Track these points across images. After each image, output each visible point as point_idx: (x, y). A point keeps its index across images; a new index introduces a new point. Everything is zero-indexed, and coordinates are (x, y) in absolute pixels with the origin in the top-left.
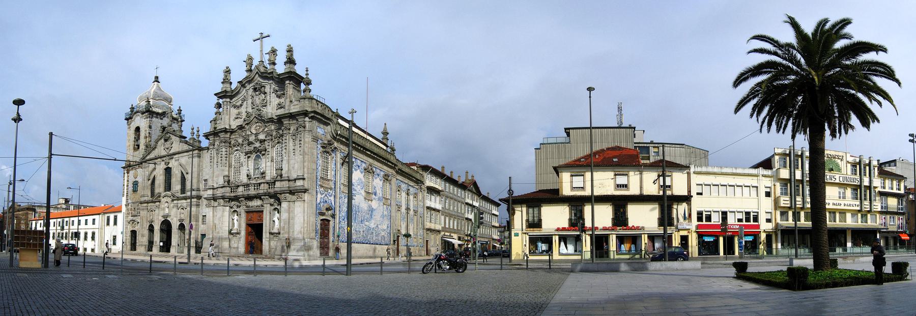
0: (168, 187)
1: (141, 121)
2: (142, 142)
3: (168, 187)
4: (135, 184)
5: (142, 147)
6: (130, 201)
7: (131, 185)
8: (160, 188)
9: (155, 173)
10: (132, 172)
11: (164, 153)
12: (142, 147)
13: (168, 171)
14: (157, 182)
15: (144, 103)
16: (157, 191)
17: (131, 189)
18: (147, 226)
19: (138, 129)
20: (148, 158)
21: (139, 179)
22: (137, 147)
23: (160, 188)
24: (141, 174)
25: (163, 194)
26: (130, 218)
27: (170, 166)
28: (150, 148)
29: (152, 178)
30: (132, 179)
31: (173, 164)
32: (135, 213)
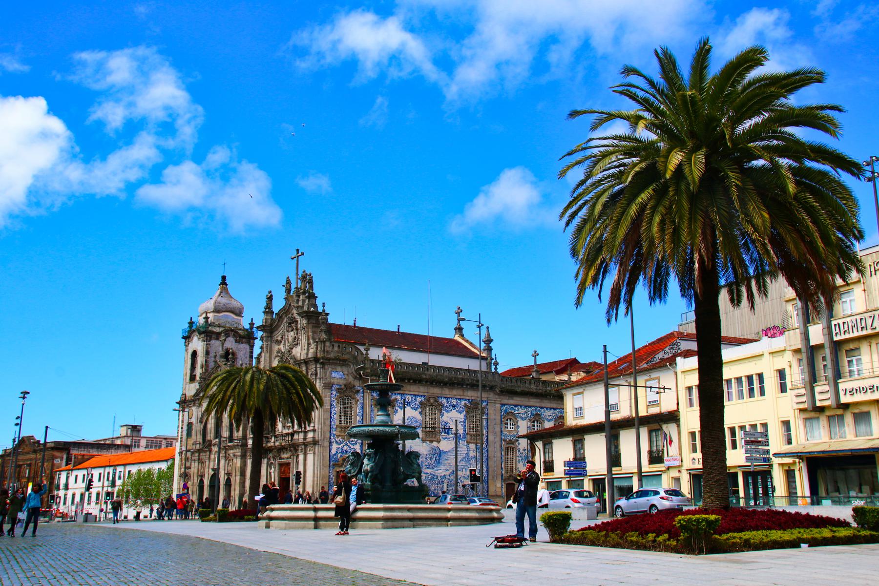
1: (197, 344)
2: (199, 371)
4: (190, 425)
7: (185, 428)
8: (210, 436)
10: (187, 410)
12: (198, 378)
14: (209, 426)
15: (201, 321)
16: (208, 438)
17: (185, 432)
18: (196, 480)
19: (194, 354)
21: (193, 420)
22: (192, 378)
23: (210, 436)
24: (196, 412)
25: (214, 442)
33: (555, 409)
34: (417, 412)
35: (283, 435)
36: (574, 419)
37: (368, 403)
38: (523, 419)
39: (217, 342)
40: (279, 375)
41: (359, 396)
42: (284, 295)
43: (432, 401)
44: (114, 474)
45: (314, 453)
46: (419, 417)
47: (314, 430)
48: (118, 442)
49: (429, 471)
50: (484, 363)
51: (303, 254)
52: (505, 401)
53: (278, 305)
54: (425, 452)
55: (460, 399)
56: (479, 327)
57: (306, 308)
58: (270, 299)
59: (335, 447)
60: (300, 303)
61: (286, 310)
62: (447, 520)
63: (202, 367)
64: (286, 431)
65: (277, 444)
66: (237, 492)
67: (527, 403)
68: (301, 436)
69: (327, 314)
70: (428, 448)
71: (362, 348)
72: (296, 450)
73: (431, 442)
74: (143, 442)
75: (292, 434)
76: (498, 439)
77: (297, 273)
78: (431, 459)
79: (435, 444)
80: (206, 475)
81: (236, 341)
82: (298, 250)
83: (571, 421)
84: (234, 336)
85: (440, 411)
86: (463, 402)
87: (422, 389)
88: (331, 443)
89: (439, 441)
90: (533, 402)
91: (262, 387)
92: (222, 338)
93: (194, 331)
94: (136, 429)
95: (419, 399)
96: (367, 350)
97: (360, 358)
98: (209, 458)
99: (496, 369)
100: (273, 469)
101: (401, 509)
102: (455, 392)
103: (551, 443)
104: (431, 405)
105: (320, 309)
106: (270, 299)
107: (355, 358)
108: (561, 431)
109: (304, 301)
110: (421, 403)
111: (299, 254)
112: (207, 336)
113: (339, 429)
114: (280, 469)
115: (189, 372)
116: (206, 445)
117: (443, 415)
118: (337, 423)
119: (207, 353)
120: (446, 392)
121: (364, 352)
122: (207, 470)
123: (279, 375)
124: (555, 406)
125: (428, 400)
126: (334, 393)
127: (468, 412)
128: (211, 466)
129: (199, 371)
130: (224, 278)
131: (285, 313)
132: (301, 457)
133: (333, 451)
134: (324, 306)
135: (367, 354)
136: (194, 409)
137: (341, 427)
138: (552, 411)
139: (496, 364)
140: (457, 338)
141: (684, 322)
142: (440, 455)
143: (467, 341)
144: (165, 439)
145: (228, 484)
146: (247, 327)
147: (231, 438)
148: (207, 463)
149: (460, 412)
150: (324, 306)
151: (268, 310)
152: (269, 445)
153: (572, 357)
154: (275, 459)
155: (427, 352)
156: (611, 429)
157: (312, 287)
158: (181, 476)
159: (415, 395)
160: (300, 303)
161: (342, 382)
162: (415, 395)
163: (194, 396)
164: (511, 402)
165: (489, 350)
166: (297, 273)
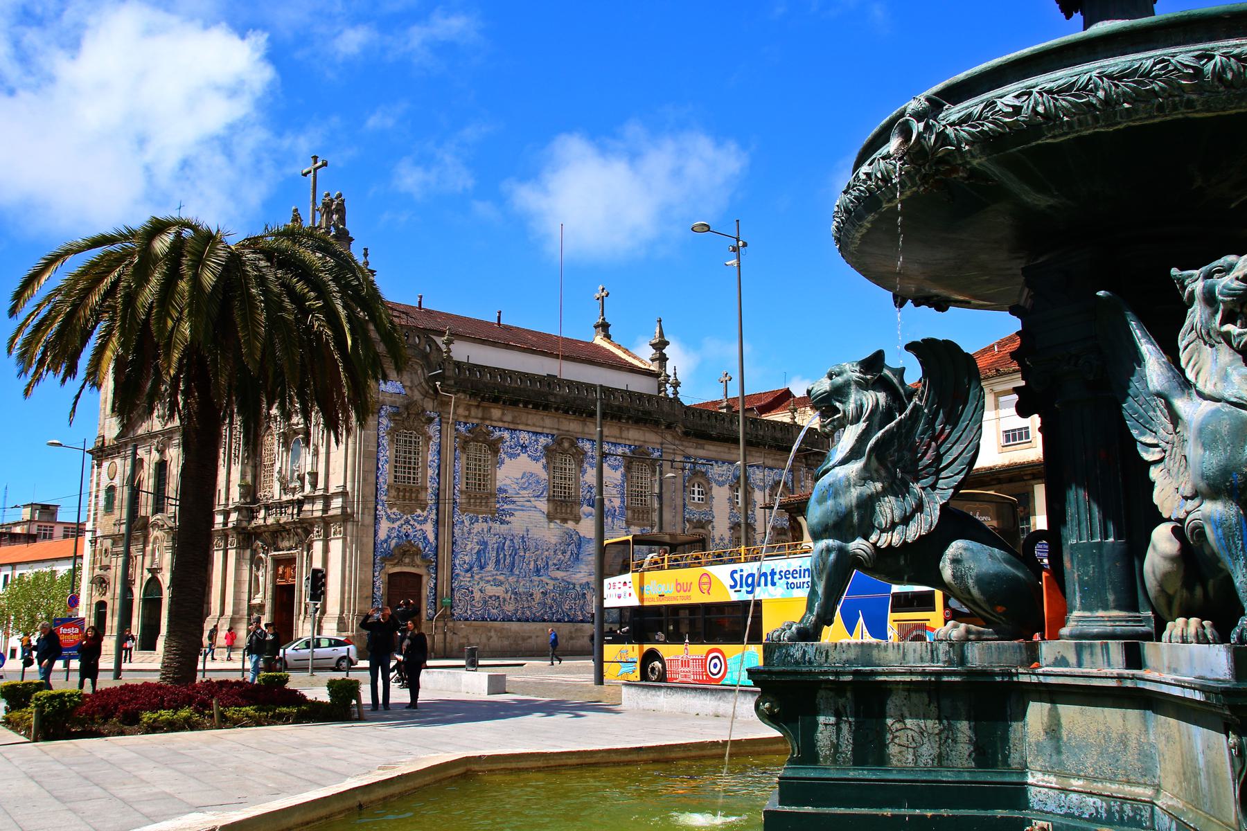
0: (159, 507)
4: (111, 490)
6: (99, 534)
7: (102, 495)
8: (146, 509)
10: (106, 464)
16: (142, 512)
17: (102, 503)
21: (117, 482)
25: (152, 520)
30: (105, 482)
33: (771, 468)
35: (281, 505)
37: (450, 443)
38: (721, 484)
40: (269, 254)
41: (432, 430)
43: (566, 445)
45: (344, 539)
46: (544, 475)
47: (344, 494)
48: (18, 530)
49: (559, 574)
51: (325, 164)
52: (691, 451)
54: (554, 540)
56: (736, 249)
59: (384, 526)
65: (270, 521)
68: (319, 506)
70: (558, 532)
71: (440, 341)
72: (308, 532)
73: (565, 520)
74: (59, 531)
75: (300, 503)
76: (679, 519)
78: (564, 552)
85: (580, 464)
87: (548, 422)
88: (376, 519)
89: (577, 520)
91: (208, 278)
95: (543, 440)
97: (434, 357)
99: (676, 393)
104: (564, 452)
107: (425, 357)
110: (546, 447)
113: (393, 493)
114: (275, 569)
117: (585, 472)
118: (391, 480)
122: (139, 571)
123: (269, 254)
124: (769, 462)
125: (560, 443)
126: (385, 421)
127: (628, 469)
128: (147, 564)
132: (318, 546)
133: (382, 535)
134: (366, 255)
135: (449, 351)
136: (118, 461)
137: (398, 490)
139: (676, 384)
140: (599, 340)
142: (579, 546)
143: (619, 347)
150: (366, 255)
153: (783, 387)
155: (557, 357)
157: (342, 219)
158: (92, 582)
159: (535, 433)
161: (399, 401)
162: (535, 433)
163: (117, 438)
164: (701, 452)
165: (662, 359)
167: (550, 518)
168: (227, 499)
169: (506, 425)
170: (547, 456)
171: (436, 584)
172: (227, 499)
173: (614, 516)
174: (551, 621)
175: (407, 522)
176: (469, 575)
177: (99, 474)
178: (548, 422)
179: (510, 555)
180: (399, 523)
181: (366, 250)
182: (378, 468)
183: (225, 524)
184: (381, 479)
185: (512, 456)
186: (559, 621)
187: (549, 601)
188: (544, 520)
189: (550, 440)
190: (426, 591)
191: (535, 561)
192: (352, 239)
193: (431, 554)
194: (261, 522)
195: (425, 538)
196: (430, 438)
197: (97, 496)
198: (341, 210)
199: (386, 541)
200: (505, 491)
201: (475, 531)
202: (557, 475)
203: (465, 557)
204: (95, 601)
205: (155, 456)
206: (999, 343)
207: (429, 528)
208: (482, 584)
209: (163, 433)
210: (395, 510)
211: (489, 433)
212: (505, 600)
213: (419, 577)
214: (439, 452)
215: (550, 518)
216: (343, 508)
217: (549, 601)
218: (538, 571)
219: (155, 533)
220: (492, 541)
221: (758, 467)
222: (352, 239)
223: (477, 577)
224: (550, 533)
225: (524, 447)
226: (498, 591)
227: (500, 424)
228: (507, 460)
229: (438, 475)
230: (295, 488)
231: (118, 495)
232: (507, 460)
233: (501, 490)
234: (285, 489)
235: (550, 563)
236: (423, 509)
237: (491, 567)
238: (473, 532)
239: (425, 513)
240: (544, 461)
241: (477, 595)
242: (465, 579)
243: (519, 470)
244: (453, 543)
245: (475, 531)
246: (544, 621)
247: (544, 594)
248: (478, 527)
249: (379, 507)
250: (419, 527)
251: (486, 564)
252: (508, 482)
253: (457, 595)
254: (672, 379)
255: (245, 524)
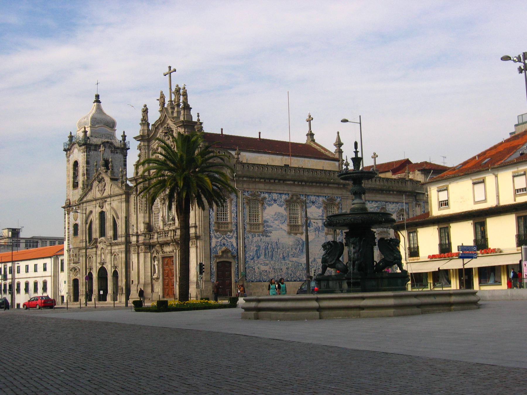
0: (103, 233)
2: (81, 179)
3: (103, 233)
4: (76, 226)
5: (80, 185)
7: (72, 229)
8: (96, 234)
9: (91, 217)
11: (99, 195)
12: (80, 185)
13: (102, 215)
15: (81, 135)
19: (76, 164)
20: (85, 199)
21: (79, 222)
22: (75, 185)
23: (96, 234)
25: (99, 240)
26: (72, 265)
27: (104, 210)
28: (88, 187)
29: (89, 222)
31: (107, 208)
32: (76, 259)
33: (397, 203)
34: (283, 208)
36: (439, 209)
39: (95, 153)
42: (159, 108)
44: (5, 269)
45: (197, 247)
49: (294, 259)
50: (337, 163)
51: (175, 71)
53: (154, 116)
54: (291, 243)
55: (318, 196)
57: (182, 118)
58: (145, 111)
59: (214, 241)
60: (175, 115)
61: (161, 122)
62: (450, 304)
63: (84, 175)
64: (166, 229)
65: (160, 240)
66: (124, 282)
67: (374, 199)
69: (201, 123)
73: (296, 234)
77: (171, 89)
78: (296, 249)
79: (299, 236)
80: (94, 269)
81: (112, 152)
82: (170, 67)
83: (436, 212)
84: (110, 147)
86: (321, 199)
88: (210, 238)
90: (379, 197)
92: (102, 149)
93: (74, 144)
94: (15, 232)
95: (284, 197)
96: (239, 154)
98: (96, 254)
100: (156, 263)
101: (387, 298)
102: (314, 190)
103: (416, 232)
105: (195, 119)
106: (145, 111)
108: (427, 221)
109: (179, 113)
111: (171, 71)
112: (87, 148)
114: (163, 262)
115: (71, 180)
116: (92, 242)
119: (88, 163)
120: (307, 190)
121: (236, 156)
122: (94, 264)
124: (396, 200)
127: (325, 208)
128: (99, 260)
129: (81, 179)
130: (97, 96)
131: (161, 124)
133: (213, 245)
134: (198, 116)
135: (238, 158)
138: (394, 205)
141: (521, 122)
144: (41, 239)
145: (115, 274)
146: (119, 137)
147: (115, 236)
148: (94, 258)
149: (319, 208)
150: (198, 116)
151: (145, 121)
152: (151, 241)
153: (406, 158)
154: (158, 252)
156: (479, 218)
157: (186, 99)
159: (280, 194)
160: (175, 115)
162: (280, 194)
166: (171, 89)
167: (289, 233)
168: (137, 229)
169: (266, 191)
170: (287, 205)
171: (238, 266)
172: (137, 229)
173: (319, 231)
174: (291, 281)
175: (224, 238)
176: (252, 261)
177: (69, 218)
178: (286, 188)
179: (271, 251)
180: (220, 239)
181: (198, 114)
182: (210, 215)
183: (137, 241)
184: (211, 220)
185: (270, 205)
186: (295, 281)
187: (290, 272)
188: (285, 234)
189: (287, 196)
190: (233, 270)
191: (283, 254)
192: (191, 108)
193: (235, 252)
194: (156, 240)
195: (232, 245)
196: (232, 200)
197: (68, 229)
198: (185, 95)
199: (215, 247)
200: (267, 222)
201: (254, 241)
202: (291, 212)
203: (251, 253)
204: (72, 279)
205: (99, 210)
206: (479, 156)
207: (234, 241)
208: (259, 265)
209: (101, 199)
210: (218, 233)
211: (259, 195)
212: (269, 272)
213: (230, 263)
214: (236, 206)
215: (289, 233)
216: (196, 233)
217: (290, 272)
218: (284, 258)
219: (100, 246)
220: (263, 245)
221: (390, 203)
222: (191, 108)
223: (256, 262)
224: (289, 240)
225: (275, 201)
226: (266, 268)
227: (263, 191)
228: (267, 207)
229: (237, 216)
230: (170, 224)
231: (79, 228)
232: (267, 207)
233: (266, 221)
234: (165, 224)
235: (290, 254)
236: (231, 232)
237: (262, 257)
238: (255, 241)
239: (232, 234)
240: (285, 206)
241: (257, 270)
242: (251, 263)
243: (273, 212)
244: (245, 247)
245: (254, 241)
246: (288, 281)
247: (287, 268)
248: (256, 239)
249: (211, 232)
250: (229, 240)
251: (260, 256)
252: (268, 217)
253: (248, 271)
254: (345, 162)
255: (147, 241)
